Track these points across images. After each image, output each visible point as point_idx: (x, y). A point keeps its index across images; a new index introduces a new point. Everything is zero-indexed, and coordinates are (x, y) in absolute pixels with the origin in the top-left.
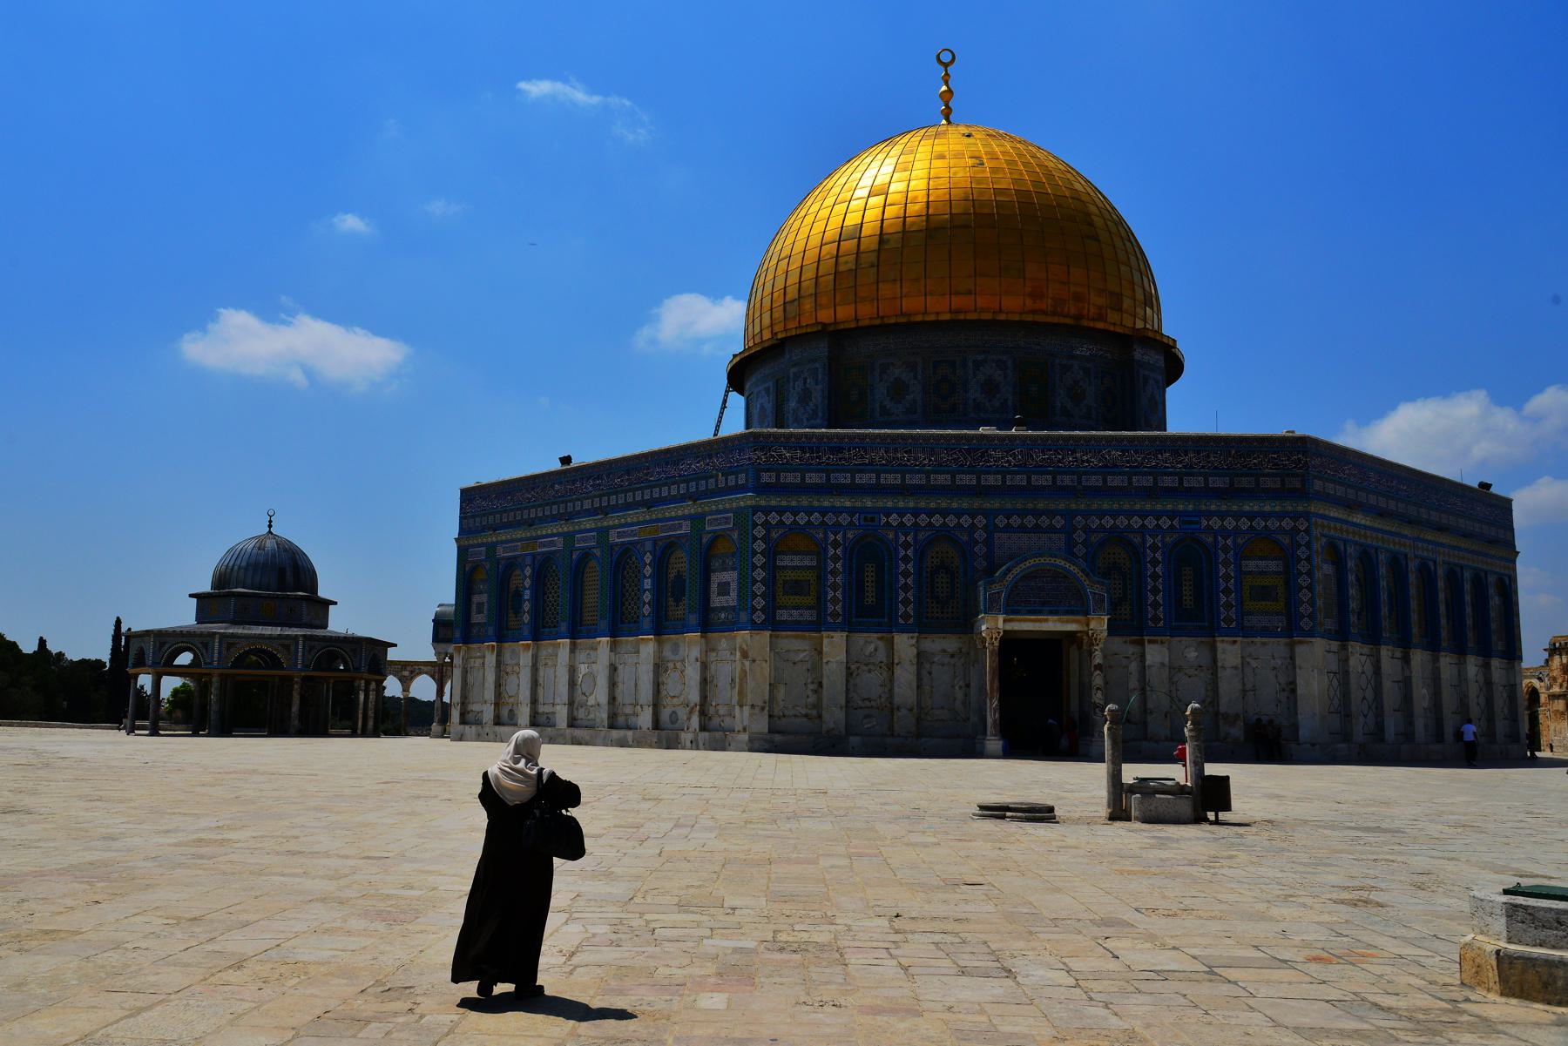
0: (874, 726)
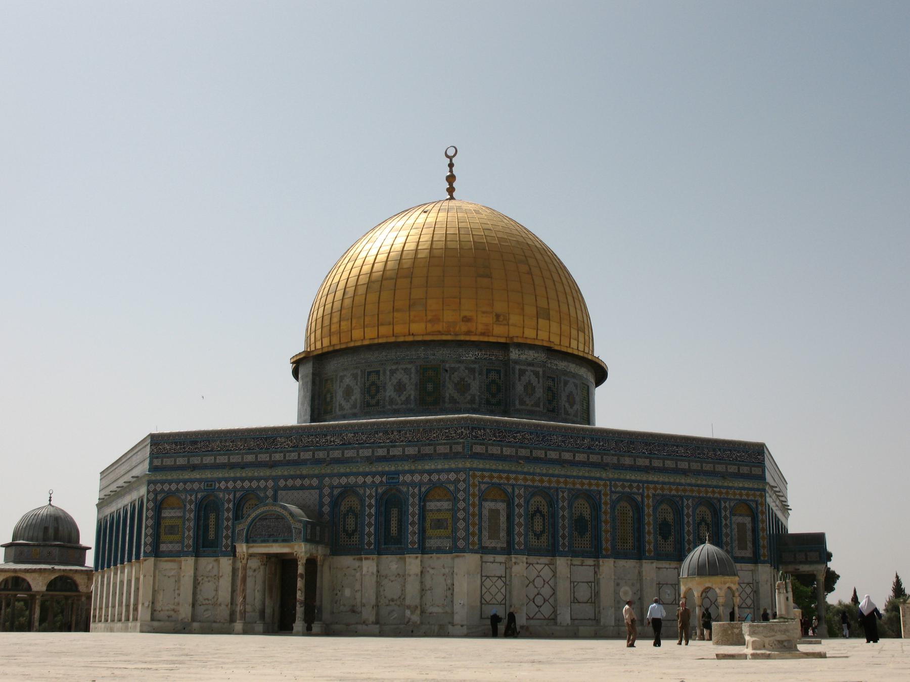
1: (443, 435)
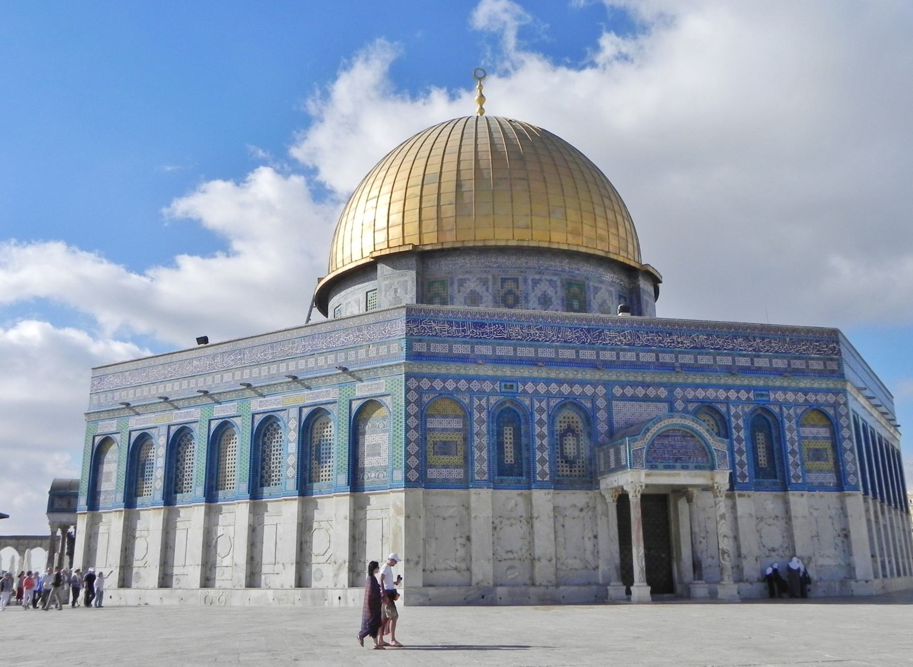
0: (518, 576)
1: (813, 348)
